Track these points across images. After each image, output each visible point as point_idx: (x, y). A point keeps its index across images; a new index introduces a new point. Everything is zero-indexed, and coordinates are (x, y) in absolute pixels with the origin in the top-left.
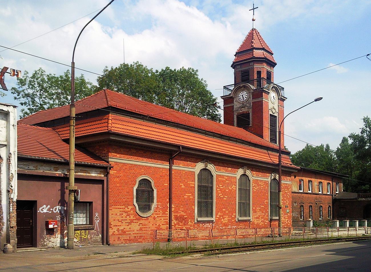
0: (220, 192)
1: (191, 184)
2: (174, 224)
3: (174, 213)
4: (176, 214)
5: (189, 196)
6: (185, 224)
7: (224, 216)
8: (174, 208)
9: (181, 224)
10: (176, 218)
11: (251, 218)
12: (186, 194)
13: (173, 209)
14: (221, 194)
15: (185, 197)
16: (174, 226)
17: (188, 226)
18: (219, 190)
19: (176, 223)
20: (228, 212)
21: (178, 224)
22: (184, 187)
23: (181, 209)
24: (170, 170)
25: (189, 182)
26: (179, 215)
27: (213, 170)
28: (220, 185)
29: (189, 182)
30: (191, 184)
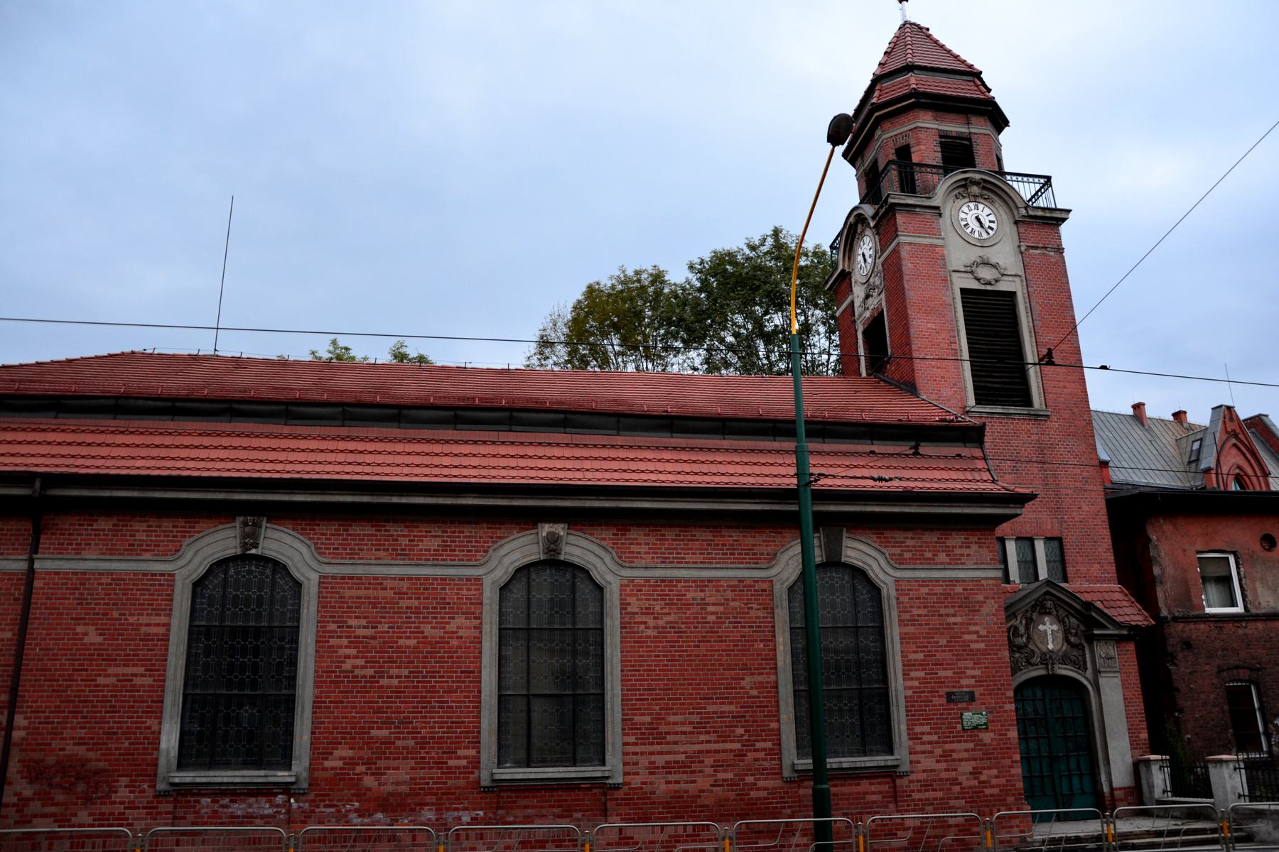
0: (353, 652)
1: (148, 625)
2: (15, 799)
3: (22, 750)
4: (37, 756)
5: (127, 679)
6: (87, 800)
7: (381, 763)
8: (25, 728)
9: (60, 798)
10: (35, 772)
11: (614, 767)
12: (111, 670)
13: (17, 735)
14: (360, 662)
15: (101, 680)
16: (14, 805)
17: (105, 809)
18: (345, 642)
19: (28, 793)
20: (411, 743)
21: (46, 798)
22: (100, 639)
23: (67, 733)
24: (31, 570)
25: (131, 619)
26: (51, 760)
27: (297, 558)
28: (352, 622)
29: (131, 619)
30: (148, 625)
